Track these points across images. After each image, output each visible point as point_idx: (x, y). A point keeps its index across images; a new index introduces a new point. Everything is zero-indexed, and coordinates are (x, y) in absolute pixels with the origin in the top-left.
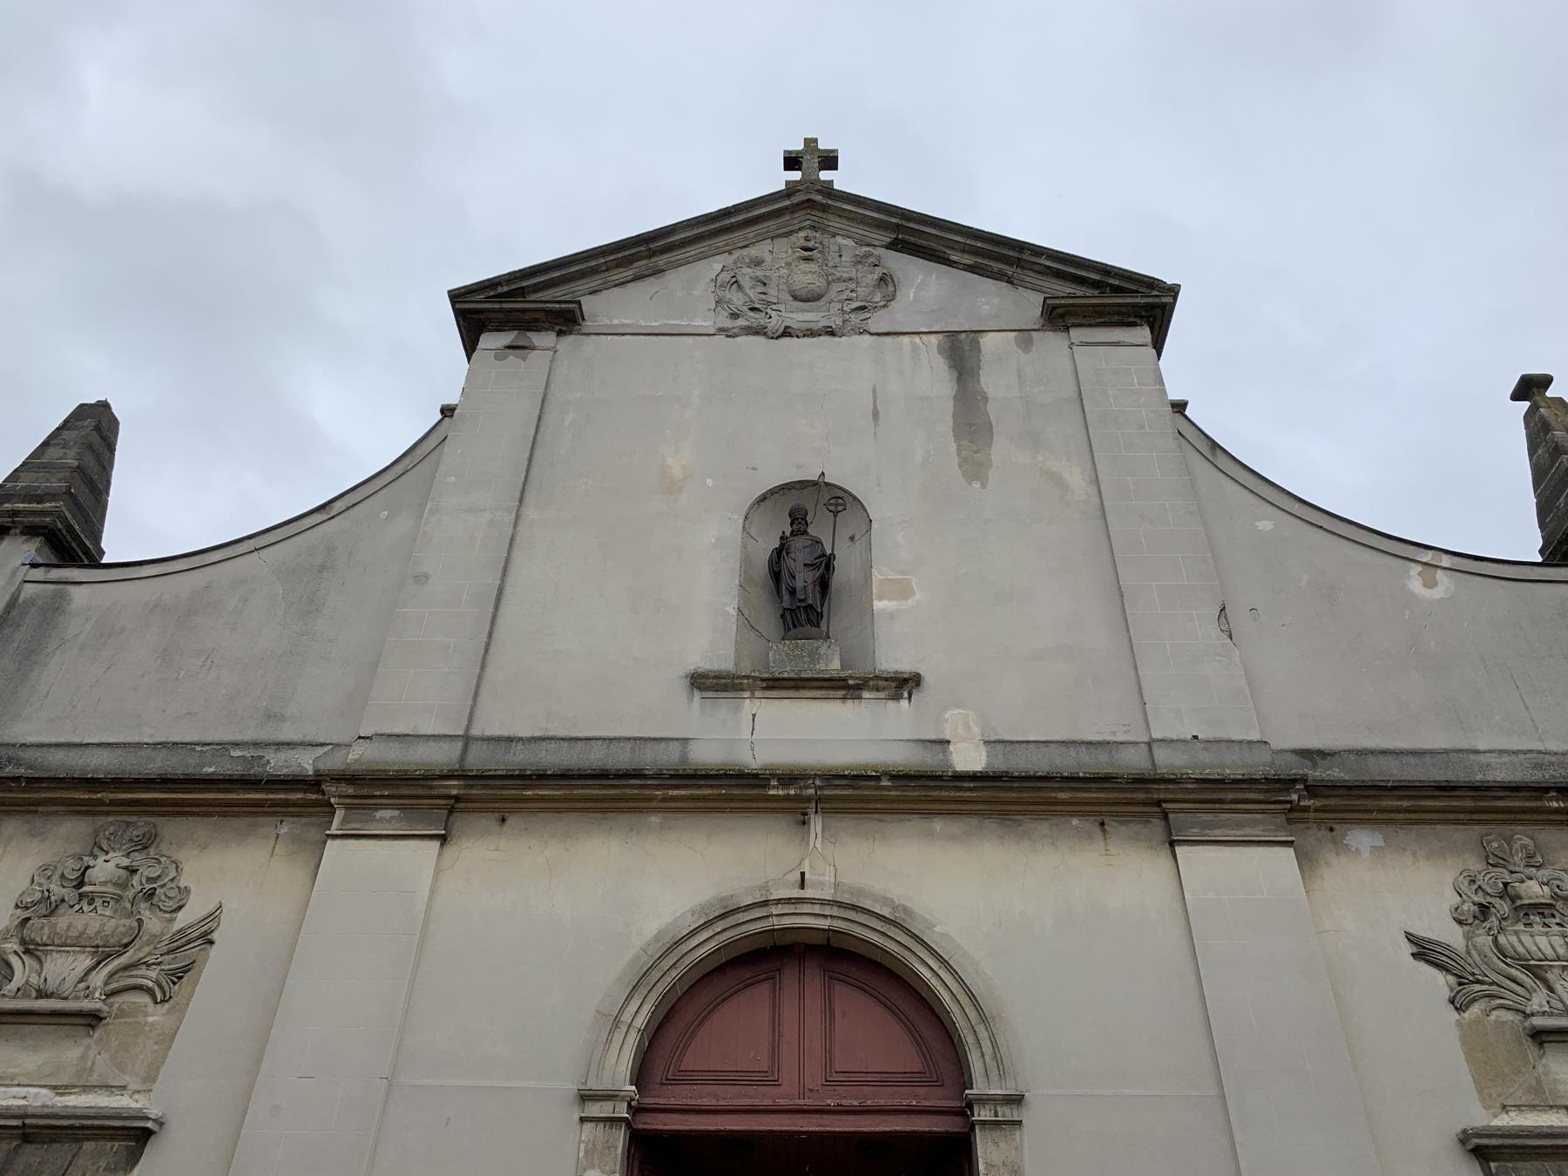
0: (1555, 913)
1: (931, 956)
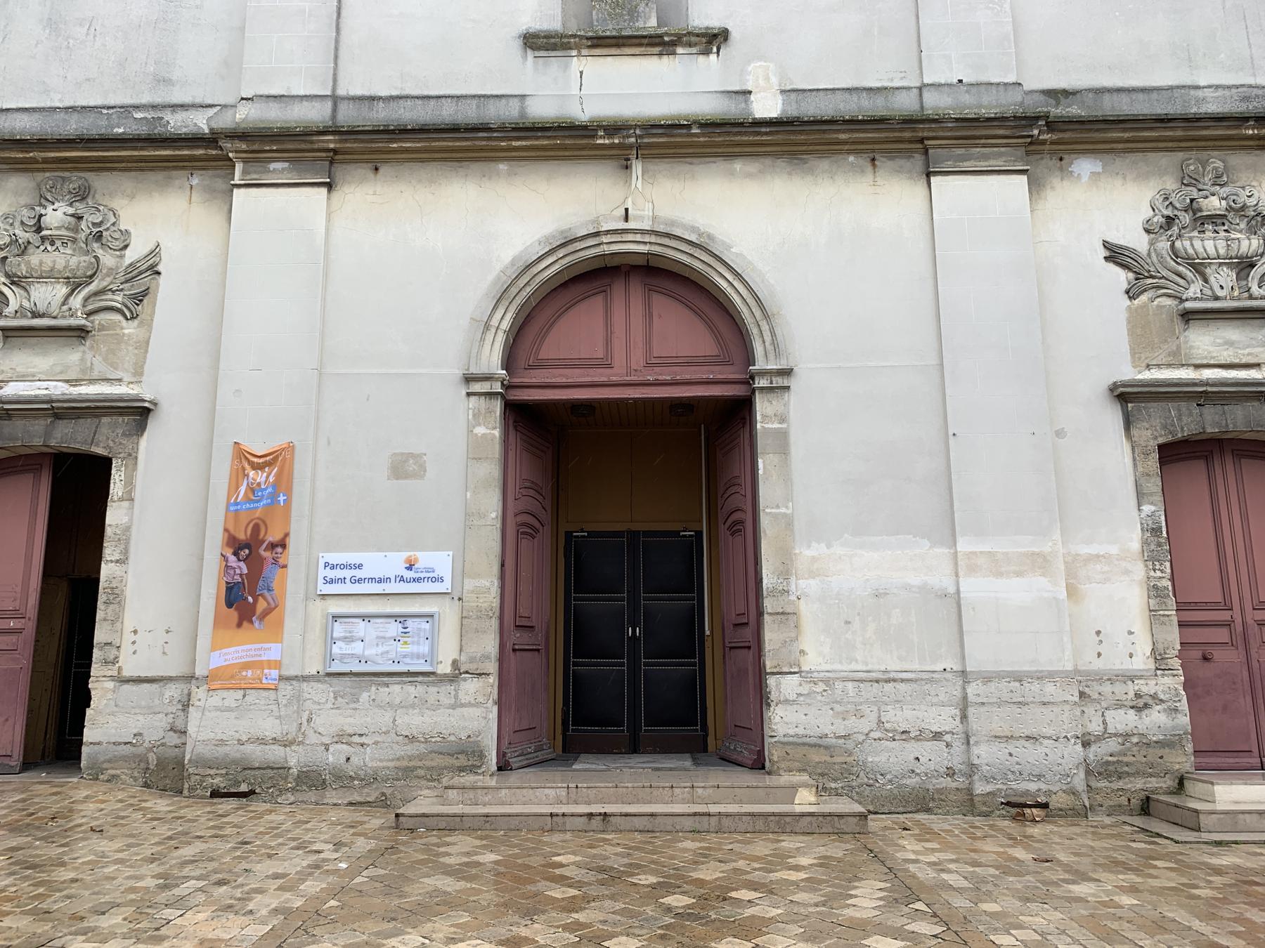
0: (1225, 221)
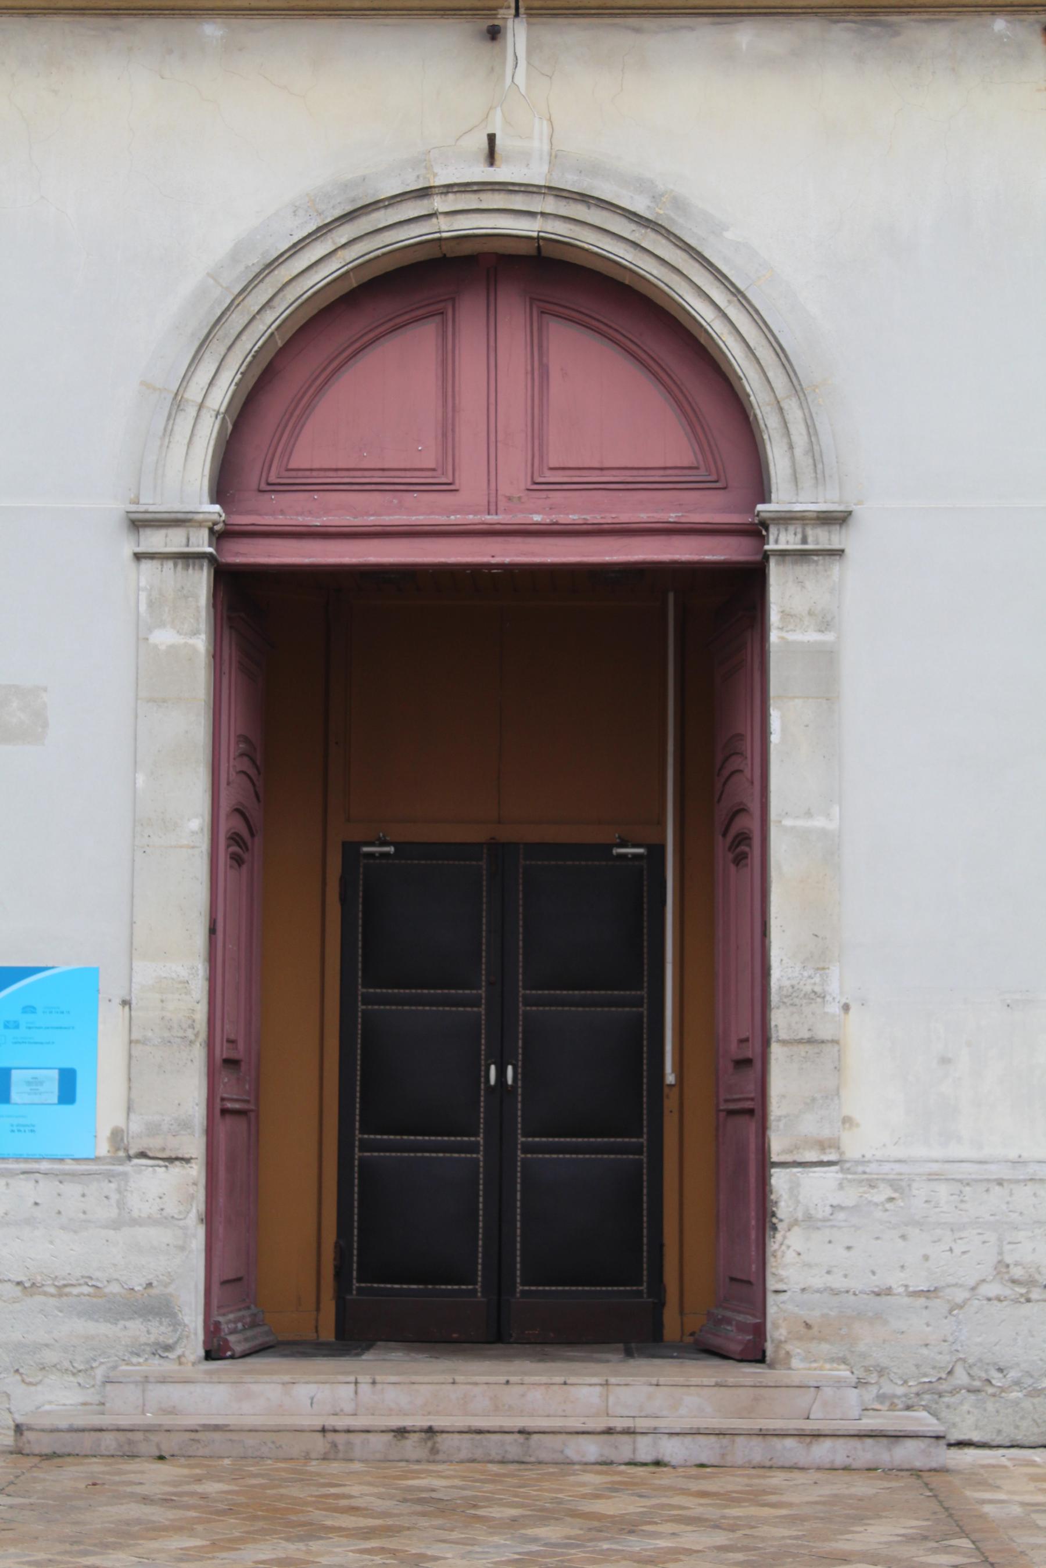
1: (718, 284)
